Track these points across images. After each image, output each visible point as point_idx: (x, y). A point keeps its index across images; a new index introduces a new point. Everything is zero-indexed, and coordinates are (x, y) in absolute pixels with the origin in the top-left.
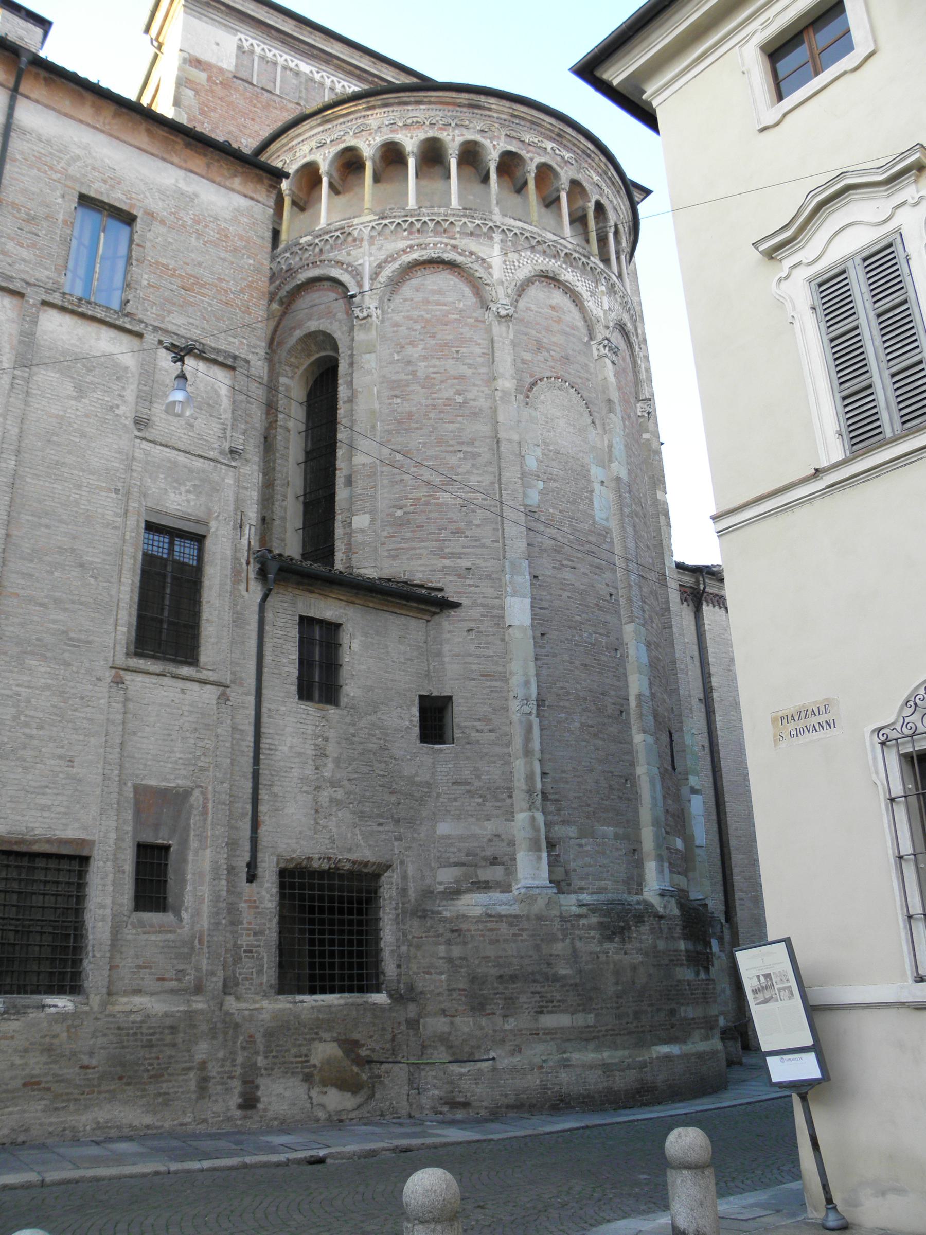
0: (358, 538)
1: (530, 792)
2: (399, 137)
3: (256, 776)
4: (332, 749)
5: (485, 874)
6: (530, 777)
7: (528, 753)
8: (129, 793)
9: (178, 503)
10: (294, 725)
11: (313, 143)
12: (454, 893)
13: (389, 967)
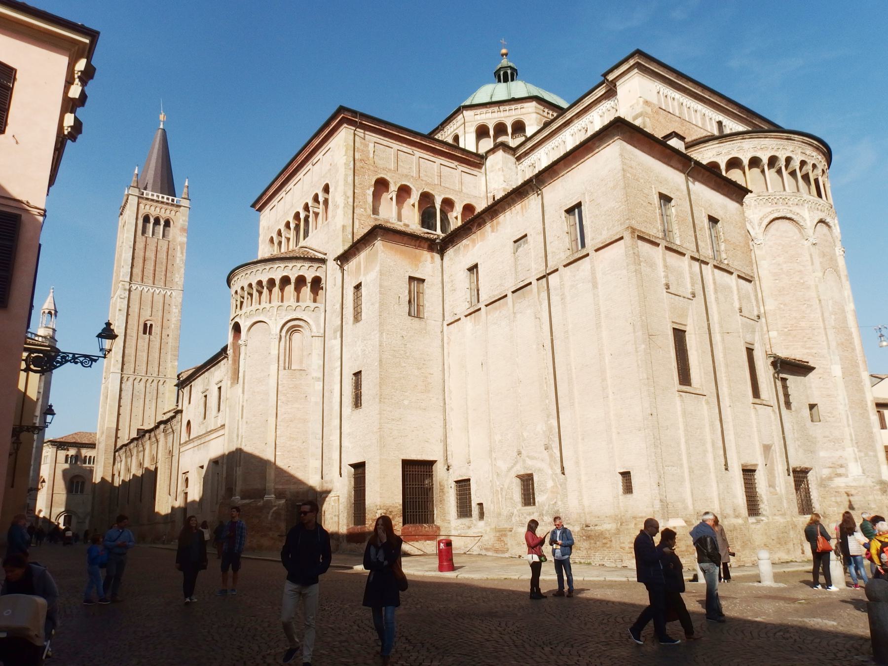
0: (773, 341)
1: (852, 440)
2: (758, 154)
5: (840, 471)
6: (851, 435)
7: (849, 426)
11: (714, 152)
12: (830, 479)
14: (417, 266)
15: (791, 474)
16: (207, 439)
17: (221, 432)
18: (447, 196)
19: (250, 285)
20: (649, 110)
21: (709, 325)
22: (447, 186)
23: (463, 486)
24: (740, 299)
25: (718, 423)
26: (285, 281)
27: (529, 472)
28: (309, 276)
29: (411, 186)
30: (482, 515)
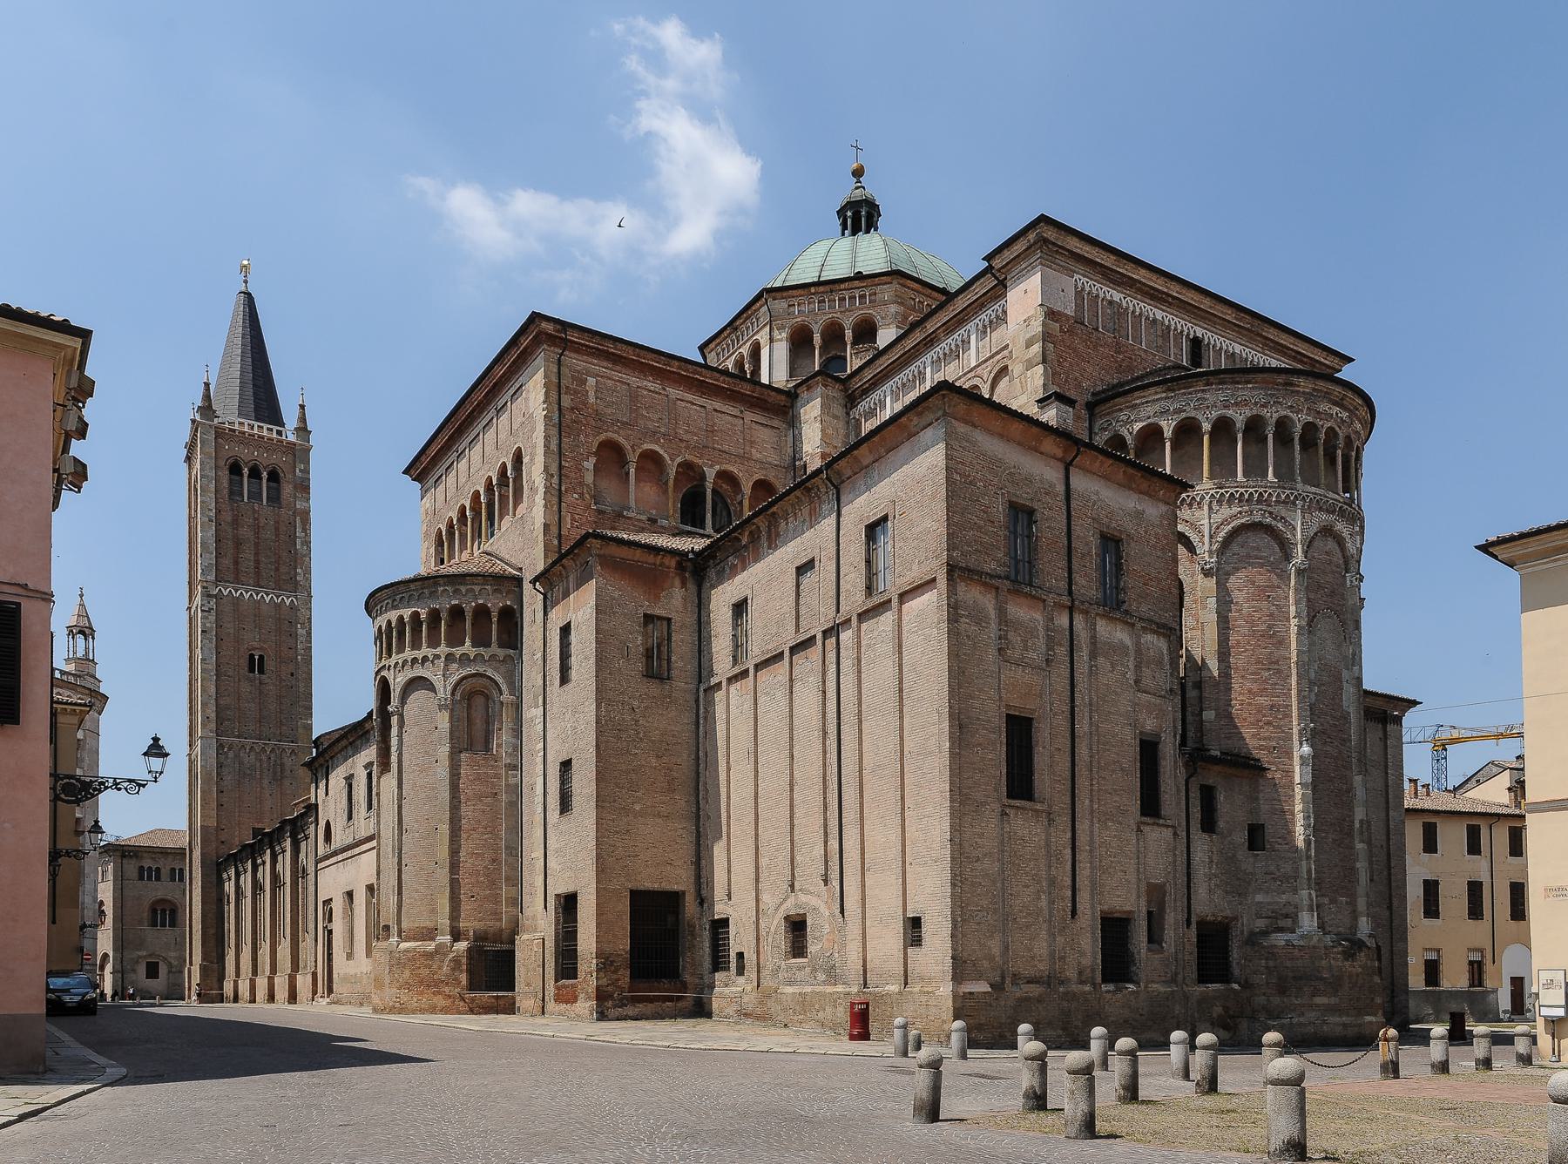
3: (1189, 875)
4: (1215, 859)
8: (1143, 888)
9: (1150, 725)
10: (1202, 845)
12: (1265, 933)
13: (1236, 972)
14: (657, 597)
15: (1194, 926)
18: (724, 467)
22: (726, 448)
24: (1138, 667)
25: (1069, 851)
29: (661, 452)
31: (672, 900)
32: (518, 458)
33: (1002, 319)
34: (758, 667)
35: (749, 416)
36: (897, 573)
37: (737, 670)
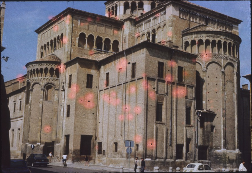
16: (15, 120)
17: (21, 118)
19: (34, 70)
20: (175, 19)
21: (147, 113)
23: (100, 144)
26: (46, 69)
27: (117, 142)
28: (55, 68)
30: (104, 154)
31: (90, 137)
32: (62, 35)
33: (165, 13)
34: (111, 88)
35: (113, 26)
36: (138, 75)
37: (106, 88)
